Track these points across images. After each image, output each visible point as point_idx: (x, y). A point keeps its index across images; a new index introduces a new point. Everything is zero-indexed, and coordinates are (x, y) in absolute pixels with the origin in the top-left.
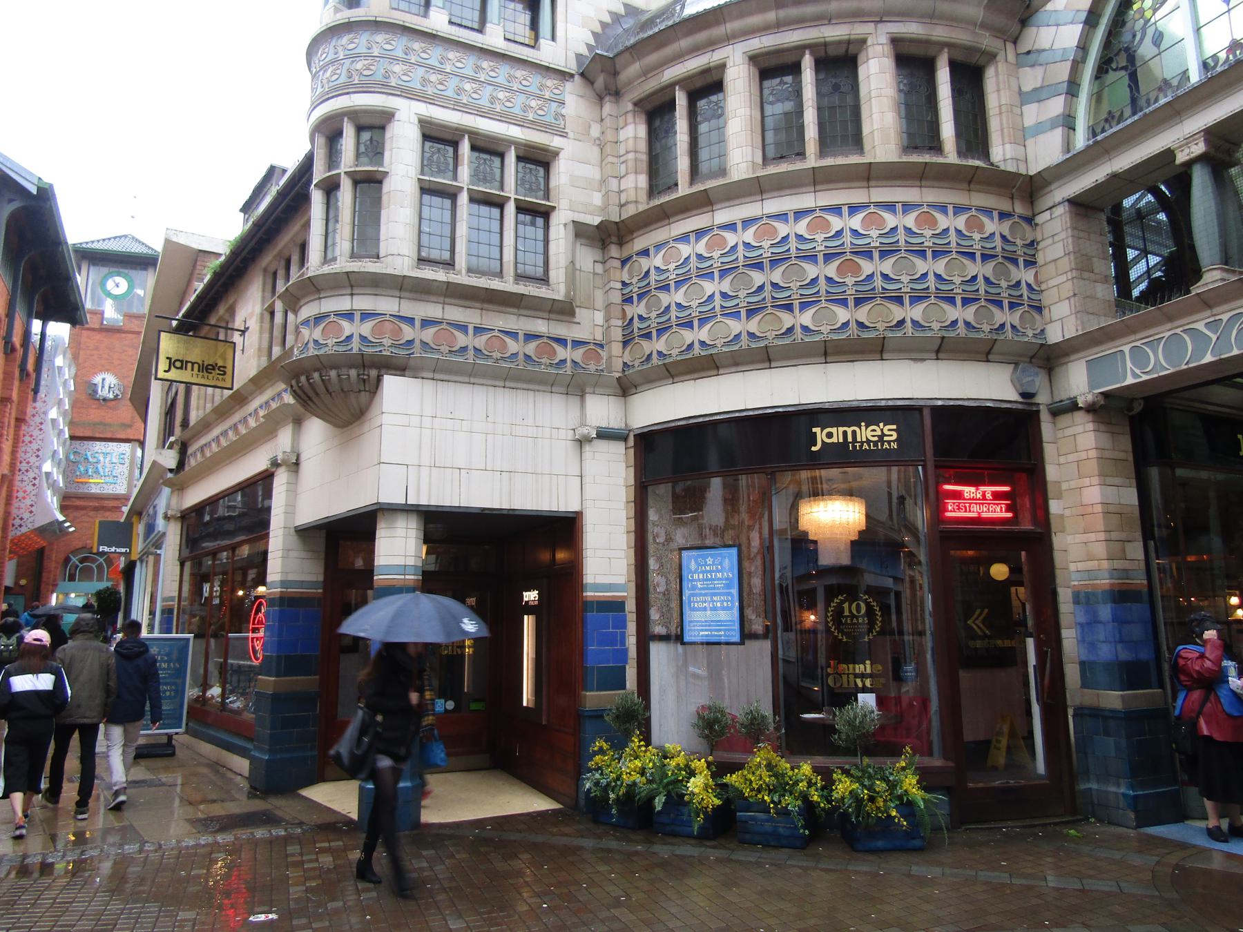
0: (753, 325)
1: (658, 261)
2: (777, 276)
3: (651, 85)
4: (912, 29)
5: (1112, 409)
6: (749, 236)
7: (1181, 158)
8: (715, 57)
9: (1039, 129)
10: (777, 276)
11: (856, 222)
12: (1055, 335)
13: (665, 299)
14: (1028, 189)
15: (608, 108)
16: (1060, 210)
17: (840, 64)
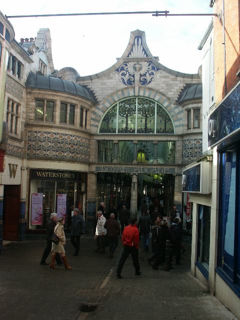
0: (57, 153)
1: (39, 135)
2: (62, 145)
3: (40, 96)
4: (84, 105)
5: (98, 175)
6: (58, 136)
7: (114, 142)
8: (55, 98)
9: (93, 125)
10: (62, 145)
11: (74, 138)
12: (91, 160)
13: (40, 143)
14: (91, 135)
15: (29, 96)
16: (95, 141)
17: (73, 106)
